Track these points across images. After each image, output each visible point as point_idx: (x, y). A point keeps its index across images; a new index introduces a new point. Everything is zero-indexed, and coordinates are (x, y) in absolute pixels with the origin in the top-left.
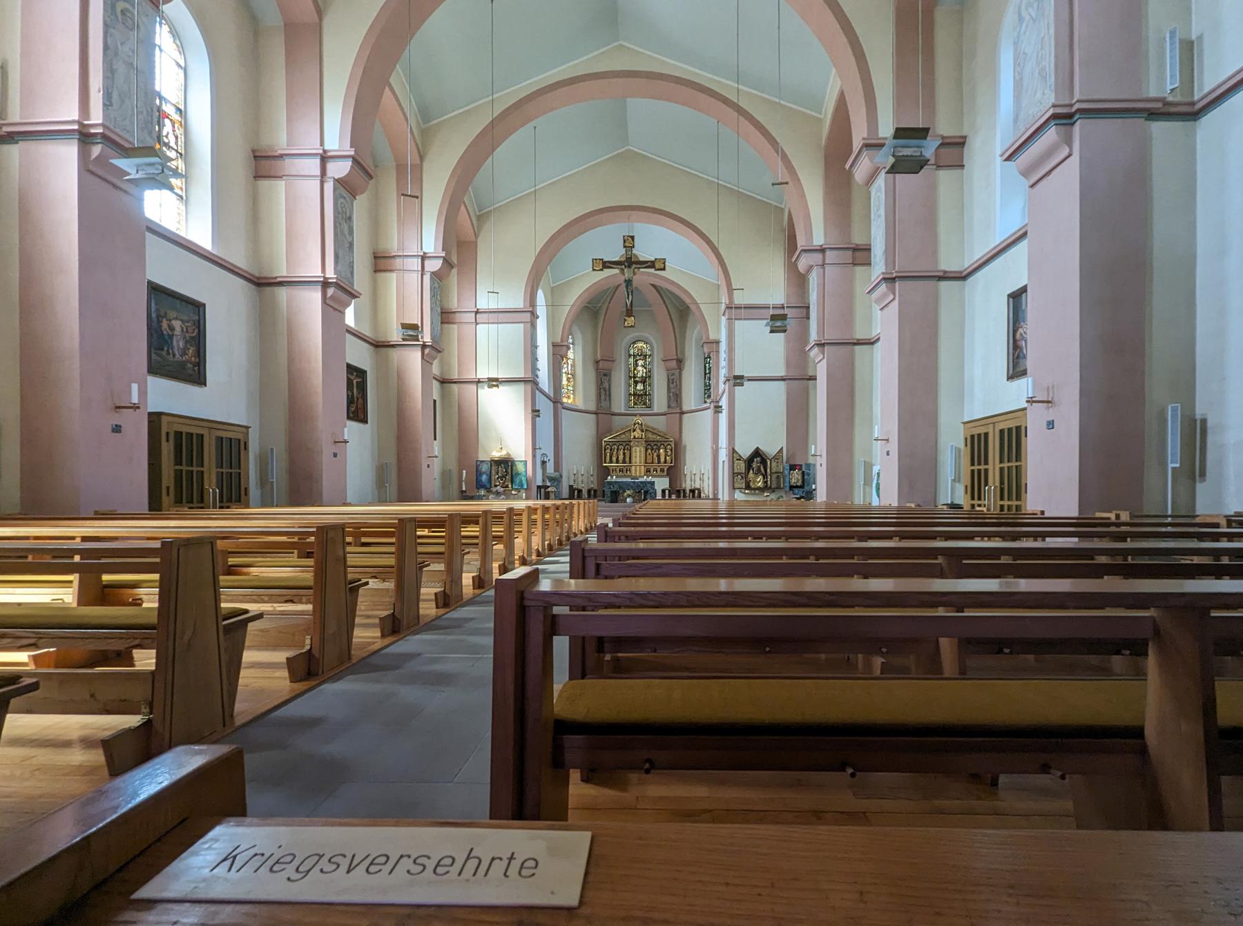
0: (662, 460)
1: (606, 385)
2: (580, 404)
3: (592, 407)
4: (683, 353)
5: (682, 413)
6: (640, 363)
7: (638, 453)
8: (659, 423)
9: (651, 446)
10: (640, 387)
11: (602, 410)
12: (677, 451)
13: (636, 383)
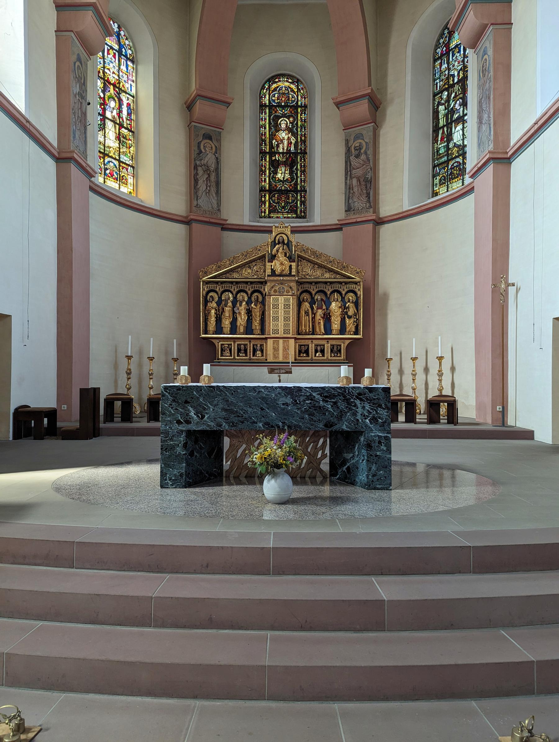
0: (336, 325)
1: (210, 159)
2: (147, 196)
3: (178, 207)
4: (383, 88)
5: (379, 222)
6: (283, 123)
7: (281, 310)
8: (329, 245)
9: (311, 294)
10: (282, 174)
11: (201, 218)
12: (367, 304)
13: (275, 165)
